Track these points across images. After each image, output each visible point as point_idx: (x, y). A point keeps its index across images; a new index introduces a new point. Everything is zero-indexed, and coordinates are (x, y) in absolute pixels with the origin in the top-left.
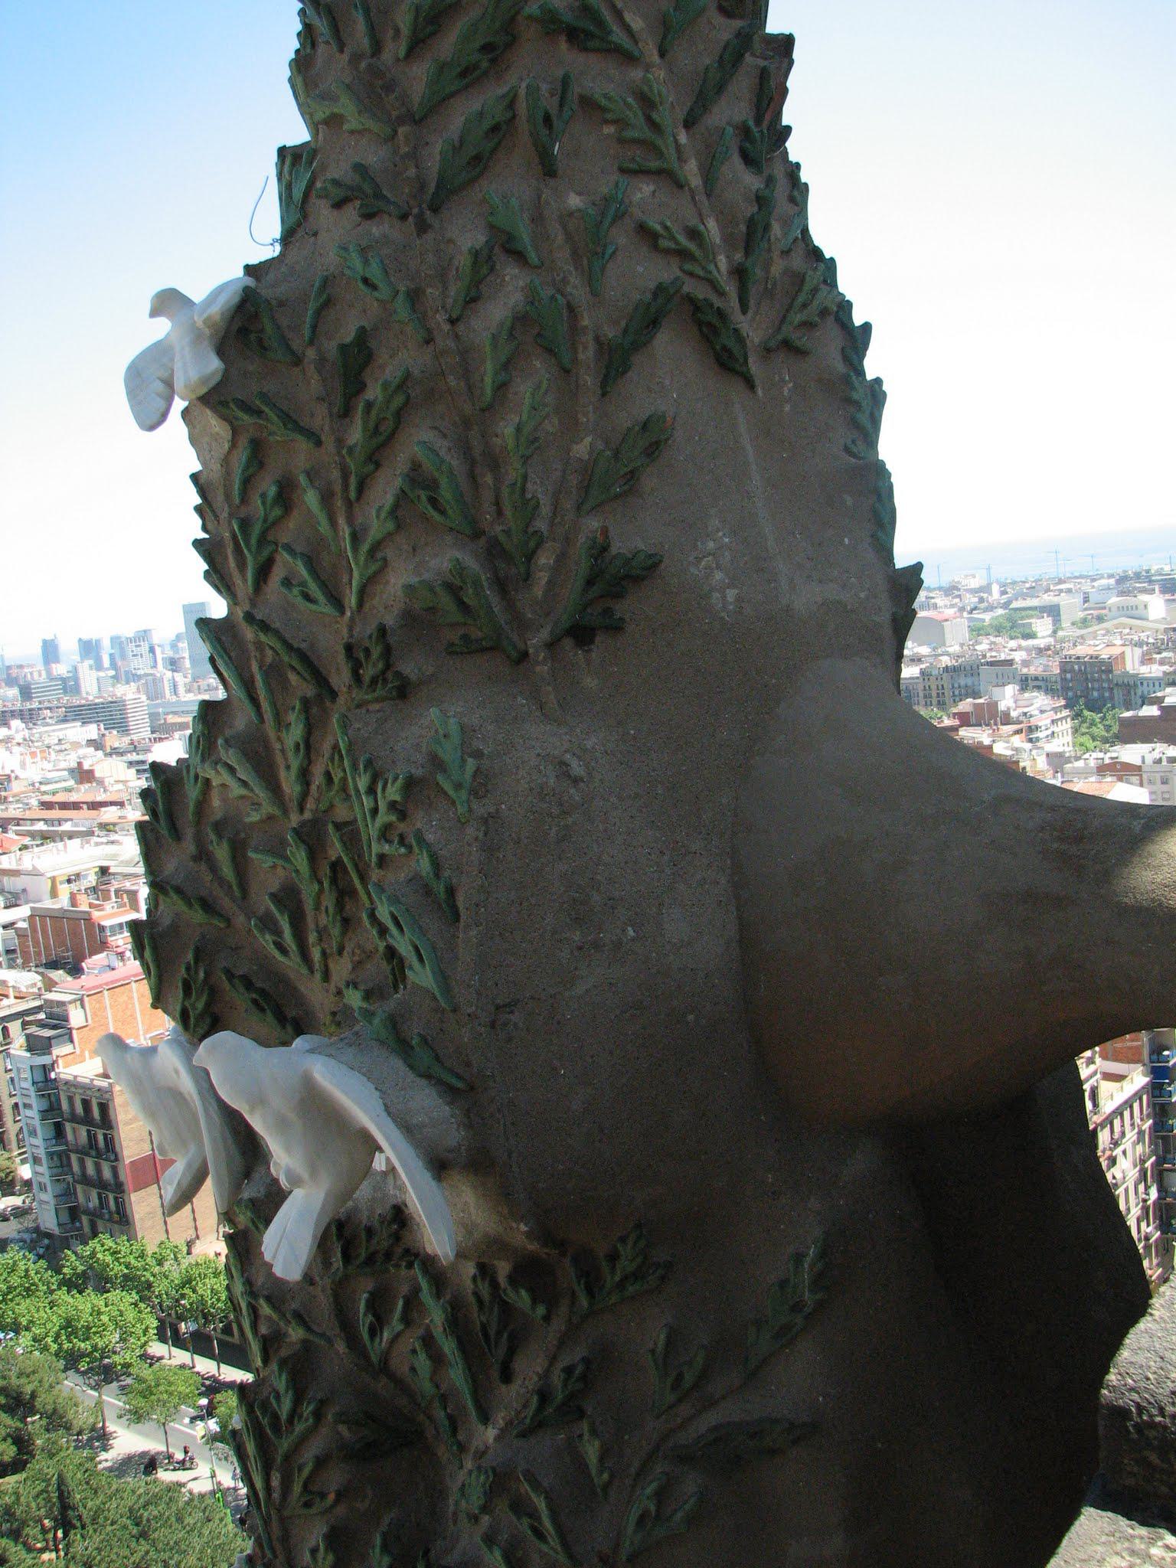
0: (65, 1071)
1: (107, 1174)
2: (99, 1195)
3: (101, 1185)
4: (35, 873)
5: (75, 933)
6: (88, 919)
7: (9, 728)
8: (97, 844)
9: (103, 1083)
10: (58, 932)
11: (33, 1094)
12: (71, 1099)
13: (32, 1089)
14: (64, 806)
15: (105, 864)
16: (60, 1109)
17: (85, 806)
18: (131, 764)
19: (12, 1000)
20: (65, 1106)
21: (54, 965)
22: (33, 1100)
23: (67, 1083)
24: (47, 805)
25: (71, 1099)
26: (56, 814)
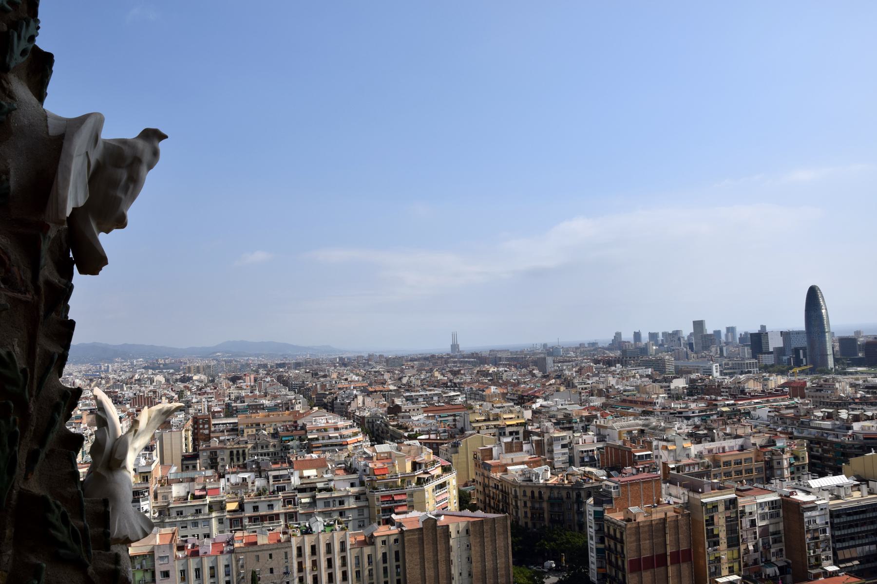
0: (607, 515)
1: (620, 563)
2: (616, 571)
3: (617, 567)
4: (612, 428)
5: (624, 457)
6: (630, 452)
7: (616, 367)
8: (640, 420)
9: (623, 523)
10: (617, 455)
11: (593, 521)
12: (609, 528)
13: (593, 520)
14: (631, 402)
15: (643, 428)
16: (604, 530)
17: (639, 403)
18: (662, 387)
19: (594, 481)
20: (606, 530)
21: (612, 469)
22: (593, 525)
23: (607, 520)
24: (624, 401)
25: (609, 528)
26: (628, 404)
